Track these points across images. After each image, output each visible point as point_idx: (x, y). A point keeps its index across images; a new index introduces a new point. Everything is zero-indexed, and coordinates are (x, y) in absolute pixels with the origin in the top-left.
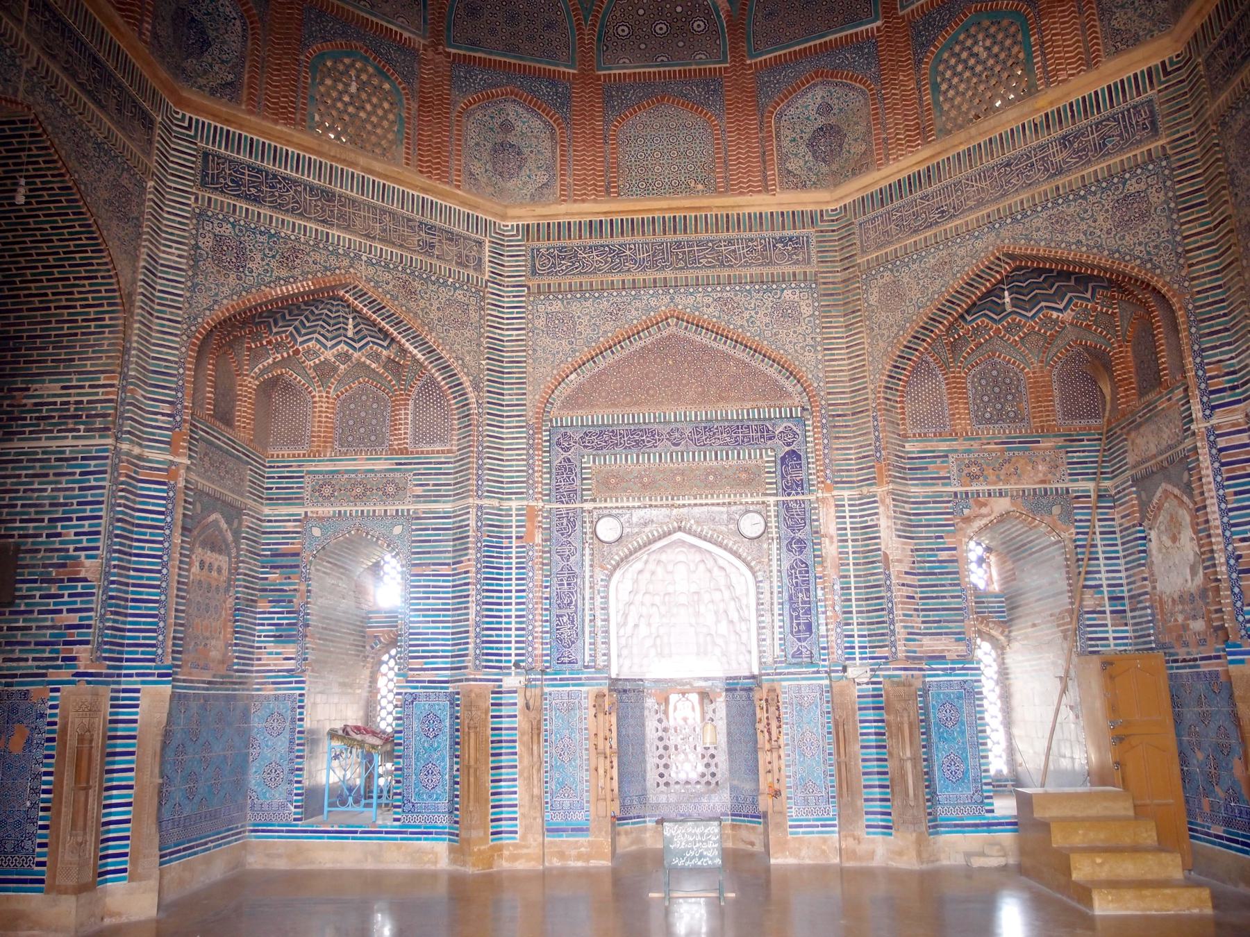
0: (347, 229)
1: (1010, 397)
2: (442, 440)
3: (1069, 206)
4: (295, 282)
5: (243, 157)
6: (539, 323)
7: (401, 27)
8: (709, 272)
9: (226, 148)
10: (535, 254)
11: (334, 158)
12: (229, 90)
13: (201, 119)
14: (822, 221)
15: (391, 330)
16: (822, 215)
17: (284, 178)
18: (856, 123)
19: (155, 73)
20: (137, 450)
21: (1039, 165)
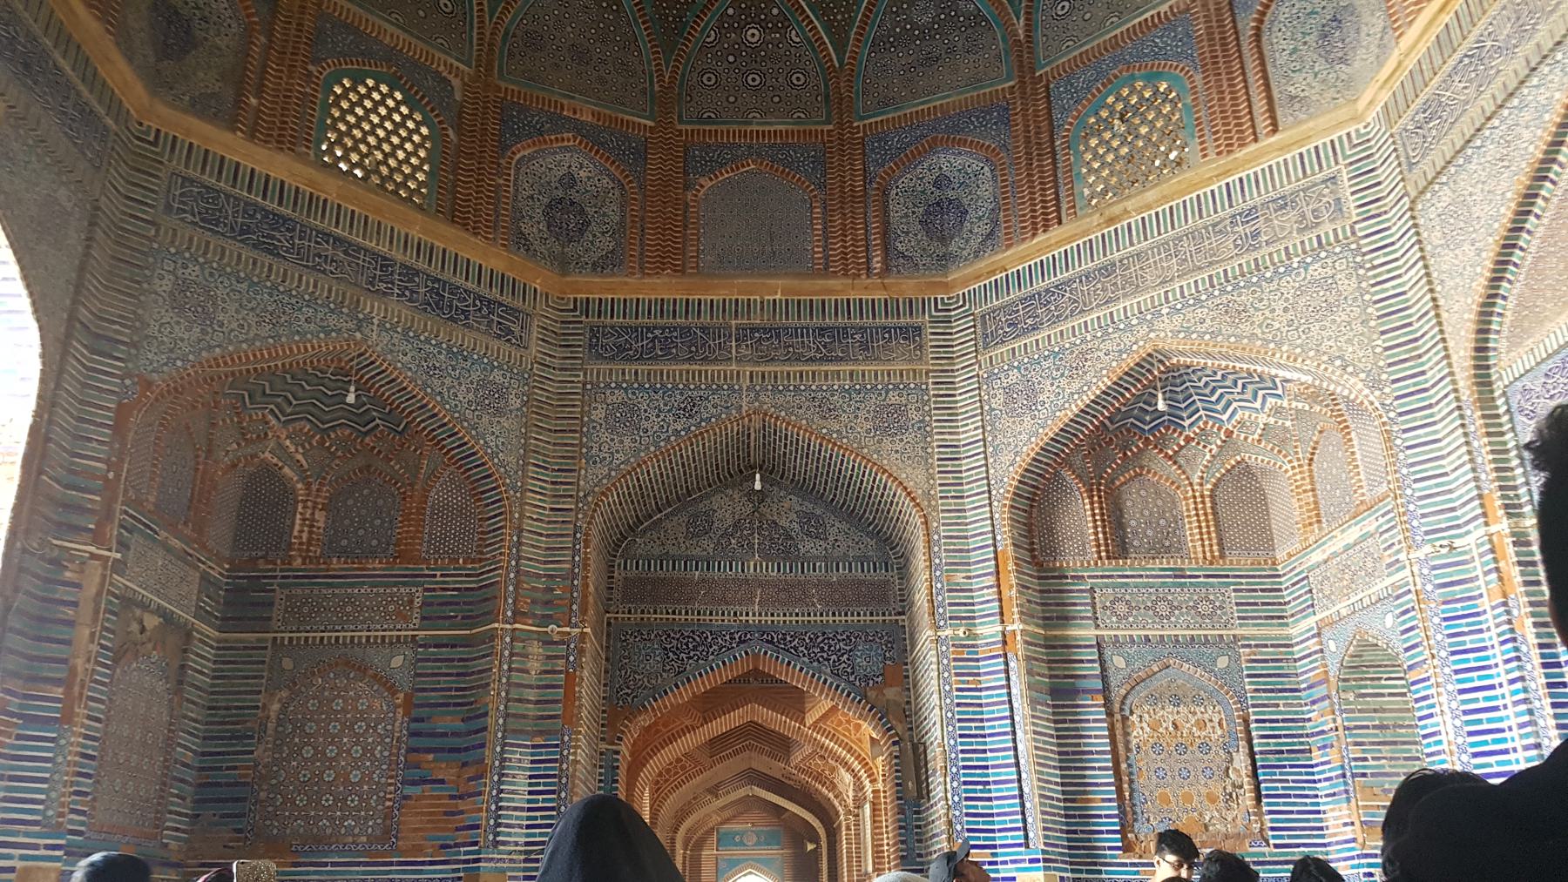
0: (1137, 290)
5: (1015, 294)
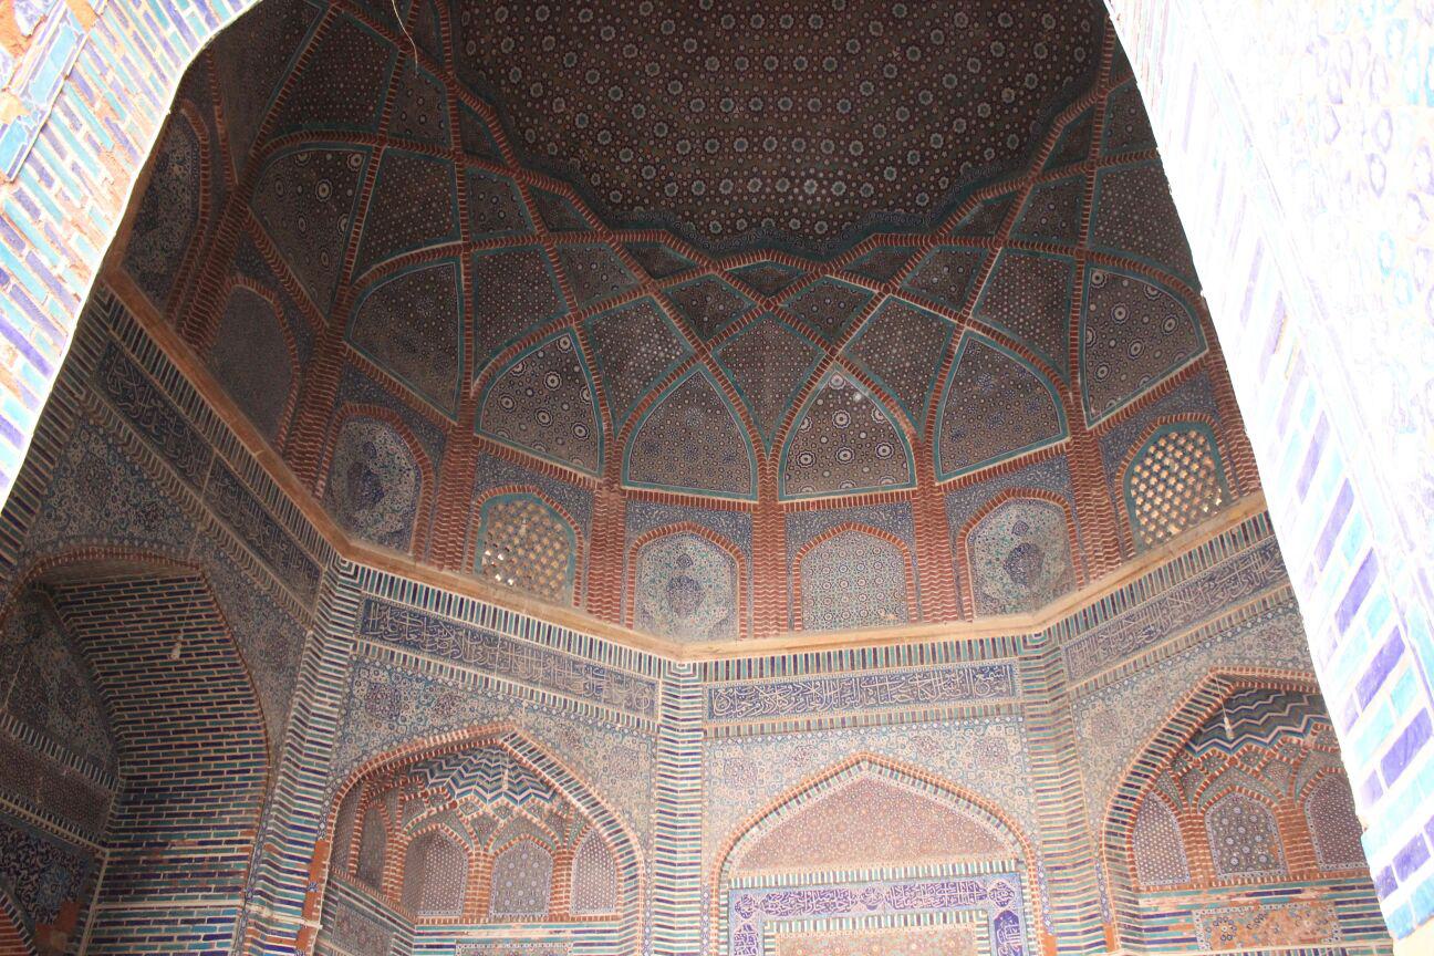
0: (508, 674)
1: (1258, 839)
2: (607, 905)
3: (1279, 620)
4: (449, 731)
5: (406, 603)
6: (717, 771)
7: (576, 468)
8: (903, 709)
9: (389, 595)
10: (713, 695)
11: (498, 601)
12: (396, 538)
13: (367, 567)
14: (1025, 647)
15: (553, 781)
16: (1025, 641)
17: (445, 623)
18: (1054, 542)
19: (323, 527)
20: (266, 913)
21: (1242, 578)
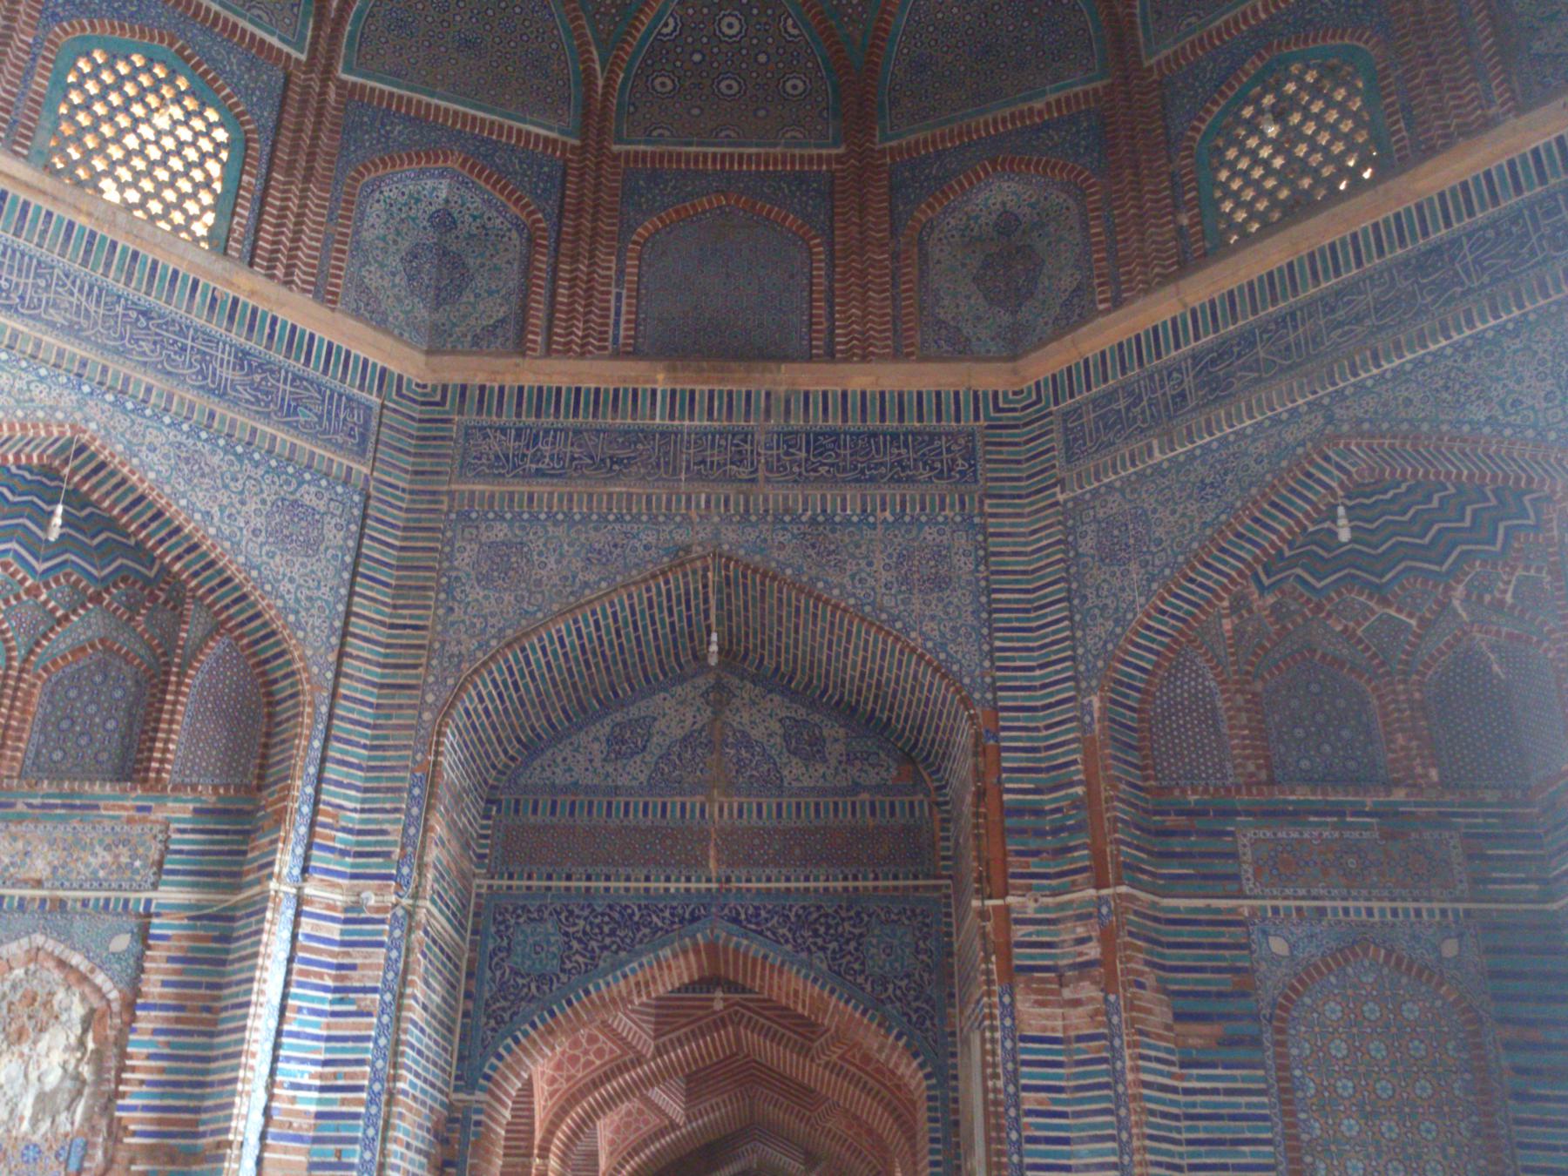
3: (213, 452)
